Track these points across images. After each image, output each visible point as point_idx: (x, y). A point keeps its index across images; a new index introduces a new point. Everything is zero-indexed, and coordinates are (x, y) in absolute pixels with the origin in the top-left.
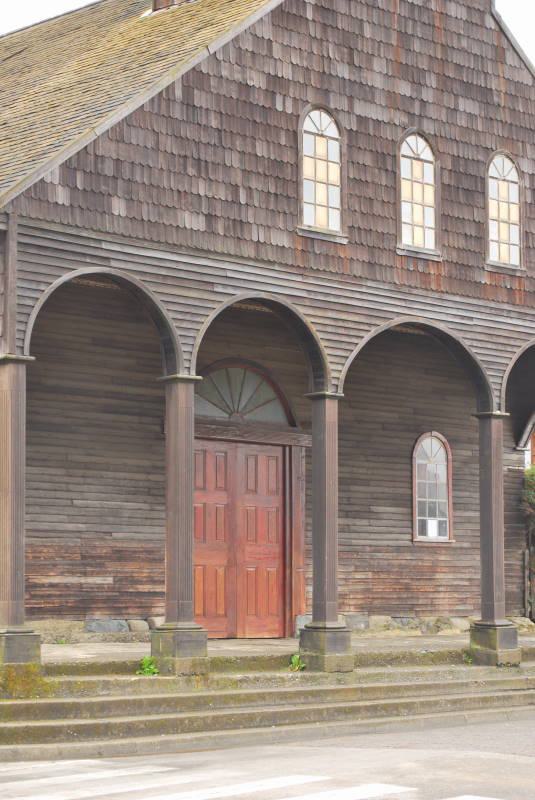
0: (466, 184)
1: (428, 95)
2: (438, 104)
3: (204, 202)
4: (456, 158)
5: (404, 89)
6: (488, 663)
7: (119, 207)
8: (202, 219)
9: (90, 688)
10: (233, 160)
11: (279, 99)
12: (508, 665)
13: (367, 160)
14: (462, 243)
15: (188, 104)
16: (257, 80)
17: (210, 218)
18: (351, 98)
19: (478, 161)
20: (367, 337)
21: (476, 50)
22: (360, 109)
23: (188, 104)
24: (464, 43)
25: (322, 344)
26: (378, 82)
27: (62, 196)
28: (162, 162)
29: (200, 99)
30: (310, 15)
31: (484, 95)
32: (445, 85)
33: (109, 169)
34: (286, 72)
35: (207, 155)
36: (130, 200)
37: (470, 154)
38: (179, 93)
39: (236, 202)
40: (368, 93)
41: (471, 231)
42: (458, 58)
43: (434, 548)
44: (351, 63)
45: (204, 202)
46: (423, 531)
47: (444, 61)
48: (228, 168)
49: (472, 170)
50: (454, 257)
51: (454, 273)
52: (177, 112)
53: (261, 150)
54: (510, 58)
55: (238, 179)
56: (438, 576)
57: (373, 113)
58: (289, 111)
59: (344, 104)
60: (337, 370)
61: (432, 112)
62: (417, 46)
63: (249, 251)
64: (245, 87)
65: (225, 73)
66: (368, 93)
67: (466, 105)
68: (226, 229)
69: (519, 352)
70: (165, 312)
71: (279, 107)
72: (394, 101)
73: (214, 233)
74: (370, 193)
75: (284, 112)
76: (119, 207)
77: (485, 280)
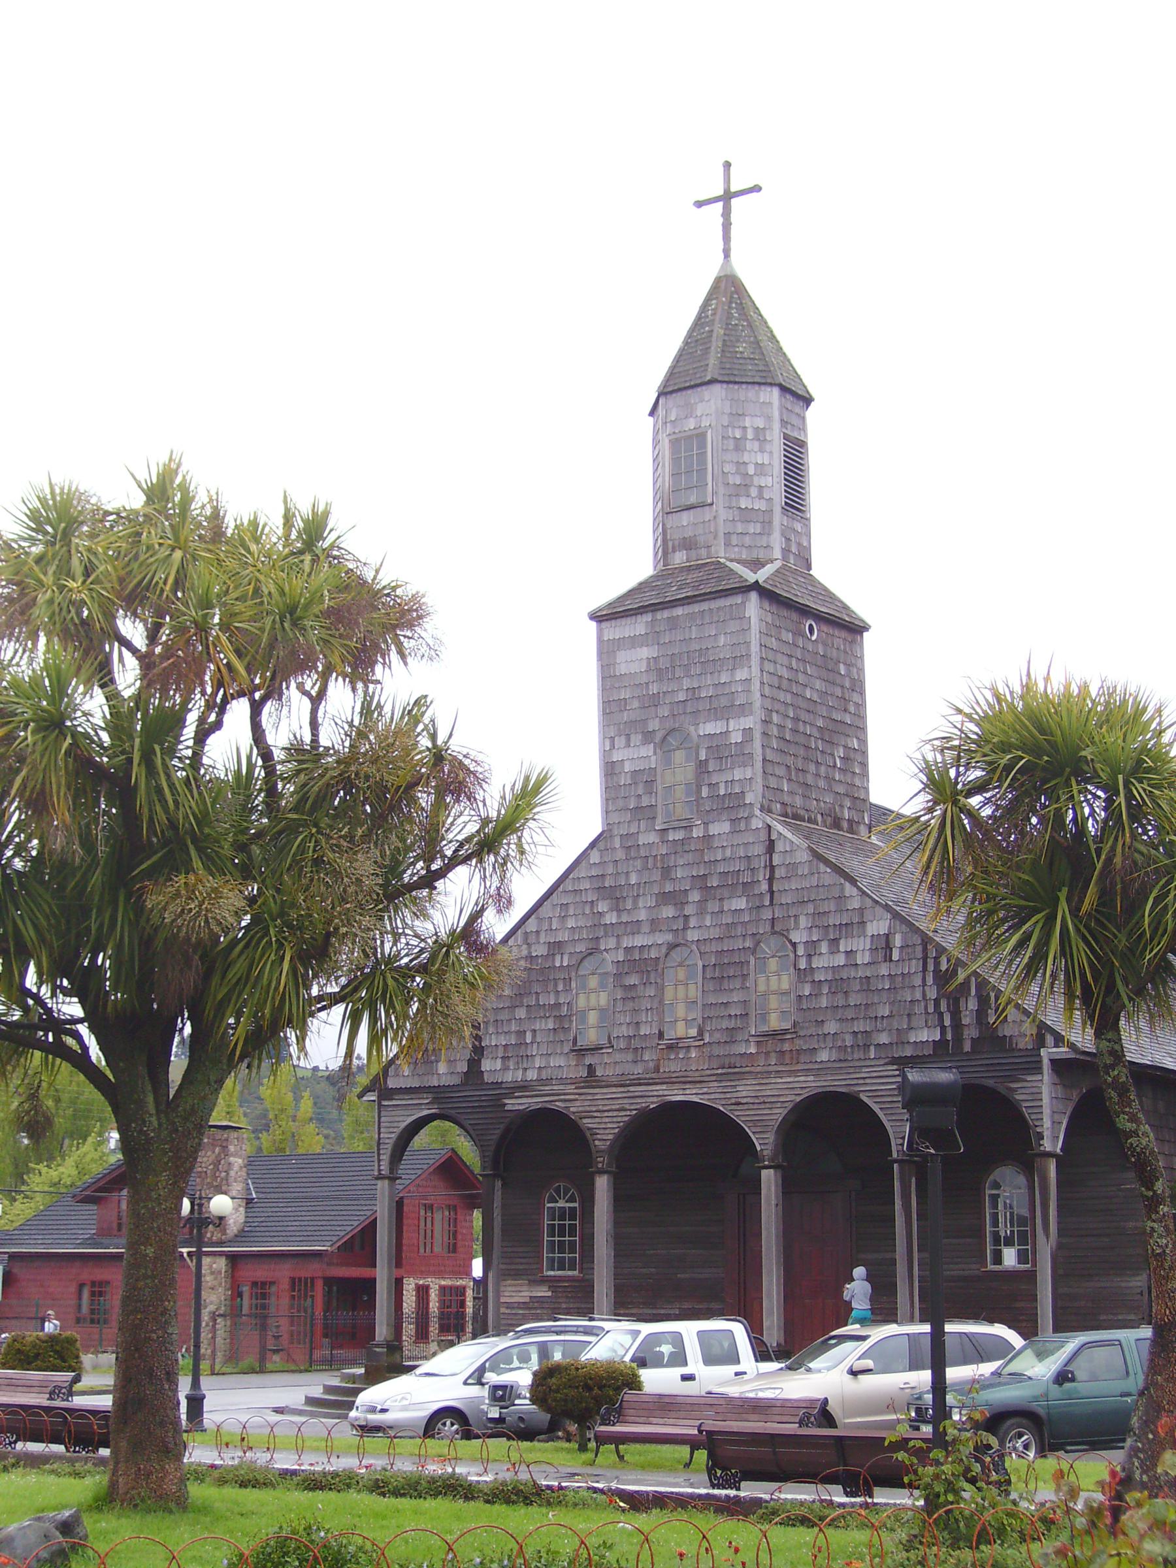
1: (689, 910)
5: (668, 912)
8: (499, 1061)
13: (633, 980)
16: (540, 950)
17: (505, 1058)
22: (627, 942)
24: (728, 853)
26: (642, 915)
34: (563, 936)
35: (504, 1016)
43: (1011, 1275)
44: (619, 911)
46: (998, 1259)
55: (525, 1027)
56: (1018, 1305)
57: (639, 941)
61: (693, 922)
64: (530, 958)
66: (634, 927)
72: (655, 925)
77: (753, 1050)
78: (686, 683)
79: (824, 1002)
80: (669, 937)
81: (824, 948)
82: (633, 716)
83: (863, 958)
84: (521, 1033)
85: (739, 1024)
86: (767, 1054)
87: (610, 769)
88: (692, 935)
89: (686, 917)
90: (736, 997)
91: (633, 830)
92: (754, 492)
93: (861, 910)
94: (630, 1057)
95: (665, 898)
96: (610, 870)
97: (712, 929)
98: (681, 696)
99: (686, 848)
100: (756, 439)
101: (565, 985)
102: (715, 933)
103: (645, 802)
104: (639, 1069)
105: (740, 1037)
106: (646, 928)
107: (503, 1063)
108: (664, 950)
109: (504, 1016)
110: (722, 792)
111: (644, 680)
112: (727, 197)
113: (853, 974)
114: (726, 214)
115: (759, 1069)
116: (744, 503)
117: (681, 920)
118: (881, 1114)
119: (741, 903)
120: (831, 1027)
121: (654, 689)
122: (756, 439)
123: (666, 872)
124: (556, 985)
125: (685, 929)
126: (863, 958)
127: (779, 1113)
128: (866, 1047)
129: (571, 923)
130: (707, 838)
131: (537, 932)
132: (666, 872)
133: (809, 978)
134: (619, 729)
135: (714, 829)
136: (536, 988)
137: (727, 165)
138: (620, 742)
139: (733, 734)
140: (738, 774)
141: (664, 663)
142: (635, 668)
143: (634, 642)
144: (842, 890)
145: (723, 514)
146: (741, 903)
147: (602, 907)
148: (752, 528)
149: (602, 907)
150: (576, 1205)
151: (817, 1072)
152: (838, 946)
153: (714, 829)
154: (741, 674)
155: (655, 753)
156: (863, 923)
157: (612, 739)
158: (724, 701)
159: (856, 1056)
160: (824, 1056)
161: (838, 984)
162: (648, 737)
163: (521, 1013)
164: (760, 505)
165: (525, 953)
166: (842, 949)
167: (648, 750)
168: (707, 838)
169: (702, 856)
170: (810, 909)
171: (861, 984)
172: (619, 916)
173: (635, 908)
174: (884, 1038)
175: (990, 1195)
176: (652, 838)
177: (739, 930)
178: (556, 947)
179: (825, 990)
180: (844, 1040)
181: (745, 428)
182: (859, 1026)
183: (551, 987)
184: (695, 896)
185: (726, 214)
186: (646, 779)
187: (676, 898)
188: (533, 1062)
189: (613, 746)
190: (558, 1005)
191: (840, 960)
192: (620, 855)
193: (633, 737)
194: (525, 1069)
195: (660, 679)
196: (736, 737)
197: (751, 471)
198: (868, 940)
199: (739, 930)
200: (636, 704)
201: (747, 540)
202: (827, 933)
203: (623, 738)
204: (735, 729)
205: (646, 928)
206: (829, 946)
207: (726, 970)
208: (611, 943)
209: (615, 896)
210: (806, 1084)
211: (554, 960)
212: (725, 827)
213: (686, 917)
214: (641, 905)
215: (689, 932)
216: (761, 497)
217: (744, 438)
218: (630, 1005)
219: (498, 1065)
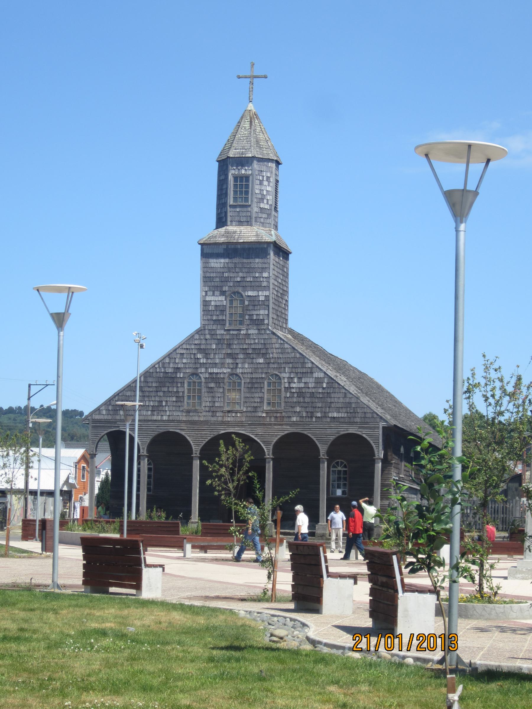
13: (212, 385)
17: (152, 411)
18: (206, 368)
19: (262, 378)
20: (209, 438)
22: (210, 370)
25: (191, 442)
26: (217, 361)
27: (104, 412)
29: (150, 380)
44: (207, 359)
50: (249, 409)
57: (215, 370)
59: (203, 370)
60: (196, 449)
61: (240, 366)
63: (165, 418)
65: (158, 370)
66: (215, 365)
69: (279, 437)
72: (222, 365)
77: (264, 415)
78: (241, 274)
79: (295, 400)
80: (229, 370)
81: (296, 380)
82: (216, 284)
85: (259, 405)
86: (270, 417)
87: (205, 304)
88: (239, 371)
89: (237, 364)
90: (257, 395)
92: (265, 201)
93: (311, 368)
94: (210, 414)
96: (204, 342)
97: (248, 369)
98: (239, 279)
99: (238, 337)
100: (267, 180)
101: (181, 385)
102: (250, 371)
103: (220, 318)
104: (213, 419)
105: (258, 409)
106: (219, 366)
107: (152, 413)
108: (227, 375)
109: (153, 394)
110: (255, 318)
111: (222, 270)
113: (307, 390)
114: (252, 83)
115: (266, 423)
116: (262, 205)
117: (235, 365)
118: (316, 441)
119: (261, 361)
120: (298, 409)
121: (226, 275)
122: (267, 180)
124: (177, 384)
125: (236, 368)
127: (275, 440)
128: (312, 417)
129: (185, 361)
130: (248, 335)
131: (169, 363)
132: (229, 345)
133: (289, 391)
134: (210, 288)
136: (168, 384)
139: (260, 297)
140: (262, 312)
141: (230, 265)
142: (218, 265)
144: (304, 360)
145: (256, 209)
146: (261, 361)
147: (199, 356)
148: (264, 216)
149: (199, 356)
150: (152, 466)
151: (290, 425)
152: (301, 380)
153: (250, 332)
154: (265, 275)
155: (226, 300)
156: (312, 373)
157: (206, 292)
158: (257, 284)
159: (307, 420)
160: (294, 419)
161: (301, 393)
162: (223, 293)
163: (161, 394)
164: (267, 207)
165: (163, 370)
166: (303, 381)
167: (222, 298)
168: (248, 335)
169: (245, 341)
170: (291, 365)
171: (310, 394)
172: (207, 360)
173: (214, 358)
174: (319, 415)
175: (332, 471)
176: (223, 332)
177: (260, 371)
179: (296, 395)
180: (303, 414)
181: (263, 176)
182: (309, 409)
183: (175, 385)
184: (241, 356)
185: (252, 83)
186: (221, 309)
188: (166, 413)
189: (206, 295)
190: (178, 392)
191: (302, 385)
192: (208, 337)
193: (216, 292)
194: (162, 416)
195: (230, 272)
196: (262, 298)
197: (265, 193)
198: (314, 379)
199: (260, 371)
200: (218, 280)
201: (262, 220)
202: (297, 375)
203: (212, 292)
204: (262, 295)
205: (219, 366)
206: (298, 380)
208: (203, 370)
209: (206, 353)
210: (288, 430)
211: (176, 375)
212: (256, 332)
213: (237, 364)
214: (217, 357)
215: (238, 369)
216: (267, 203)
217: (263, 180)
218: (211, 394)
219: (149, 413)
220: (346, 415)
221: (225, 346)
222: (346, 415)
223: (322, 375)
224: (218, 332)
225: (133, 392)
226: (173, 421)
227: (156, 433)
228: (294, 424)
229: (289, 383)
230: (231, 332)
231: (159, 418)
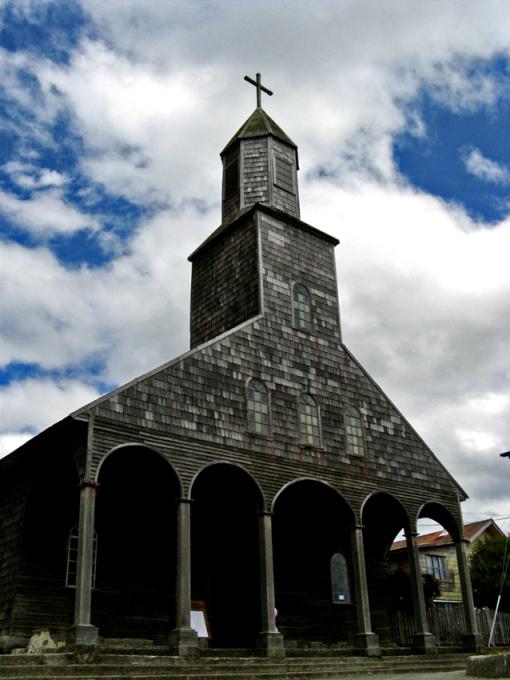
0: (333, 417)
1: (311, 377)
2: (317, 381)
3: (196, 417)
4: (328, 406)
5: (299, 373)
6: (364, 655)
7: (149, 416)
9: (127, 660)
10: (211, 399)
11: (235, 374)
12: (374, 656)
13: (282, 403)
14: (333, 444)
15: (187, 372)
17: (198, 424)
18: (272, 376)
21: (334, 359)
22: (277, 380)
23: (187, 372)
24: (328, 356)
26: (286, 370)
27: (118, 408)
28: (172, 396)
29: (192, 370)
30: (249, 338)
31: (339, 379)
32: (320, 373)
33: (144, 398)
34: (238, 362)
35: (198, 396)
36: (155, 413)
37: (336, 404)
38: (182, 367)
39: (212, 418)
40: (282, 375)
41: (338, 439)
42: (324, 362)
44: (271, 361)
45: (196, 417)
47: (319, 363)
48: (208, 403)
49: (336, 411)
51: (331, 457)
52: (181, 375)
53: (225, 395)
54: (352, 364)
55: (213, 407)
57: (284, 383)
58: (240, 378)
61: (313, 384)
62: (304, 356)
63: (219, 441)
64: (216, 366)
65: (206, 360)
66: (282, 375)
67: (331, 383)
68: (207, 430)
70: (174, 467)
71: (235, 377)
72: (293, 378)
73: (201, 432)
74: (284, 418)
75: (237, 379)
76: (149, 416)
83: (391, 432)
84: (211, 412)
89: (309, 380)
91: (279, 321)
94: (283, 448)
95: (296, 365)
112: (257, 84)
123: (298, 353)
126: (391, 432)
131: (221, 353)
135: (321, 342)
136: (220, 386)
137: (258, 76)
138: (270, 273)
142: (278, 242)
143: (277, 231)
146: (336, 384)
153: (321, 342)
160: (380, 474)
167: (285, 285)
178: (233, 367)
184: (313, 371)
187: (305, 369)
207: (332, 420)
209: (270, 352)
219: (194, 426)
220: (426, 478)
221: (293, 352)
222: (426, 478)
223: (398, 421)
224: (284, 329)
225: (166, 384)
226: (231, 448)
227: (208, 464)
228: (380, 482)
229: (369, 423)
230: (300, 335)
231: (210, 438)
